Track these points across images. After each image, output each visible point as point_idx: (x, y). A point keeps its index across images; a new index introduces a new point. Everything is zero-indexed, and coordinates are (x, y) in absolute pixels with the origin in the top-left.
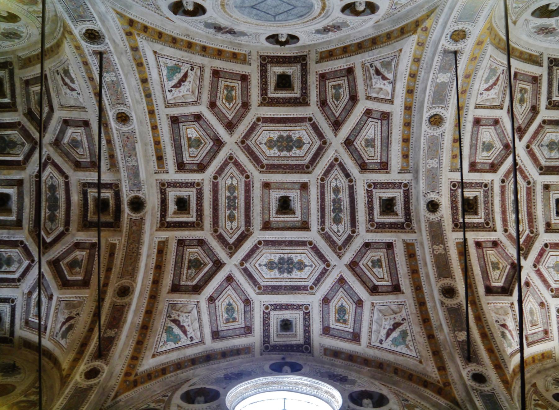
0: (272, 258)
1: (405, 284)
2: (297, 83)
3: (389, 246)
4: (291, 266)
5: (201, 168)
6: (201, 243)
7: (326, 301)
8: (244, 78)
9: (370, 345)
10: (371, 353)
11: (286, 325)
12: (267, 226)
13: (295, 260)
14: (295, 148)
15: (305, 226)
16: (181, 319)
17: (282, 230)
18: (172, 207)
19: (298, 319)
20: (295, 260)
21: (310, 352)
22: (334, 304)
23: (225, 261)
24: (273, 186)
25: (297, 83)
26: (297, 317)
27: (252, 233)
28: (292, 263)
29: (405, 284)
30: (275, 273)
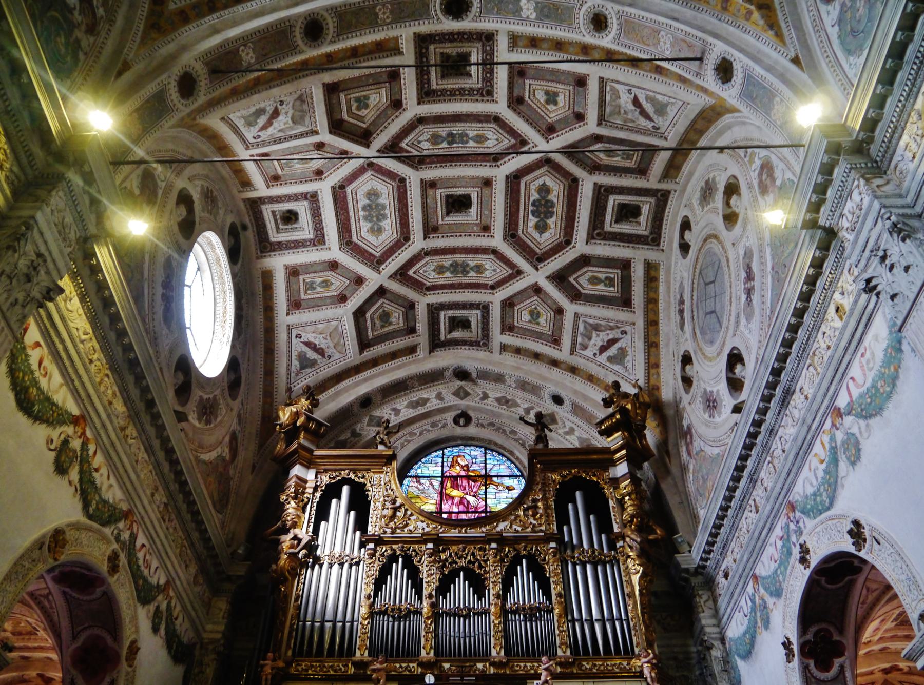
0: (384, 196)
1: (370, 353)
2: (625, 228)
3: (412, 330)
4: (375, 219)
5: (516, 102)
6: (397, 104)
7: (333, 265)
8: (642, 171)
9: (289, 329)
10: (281, 336)
11: (290, 217)
12: (428, 185)
13: (382, 224)
14: (536, 220)
15: (430, 229)
16: (281, 118)
17: (423, 203)
18: (451, 49)
19: (301, 233)
20: (382, 224)
21: (262, 252)
22: (330, 275)
23: (372, 145)
24: (486, 191)
25: (625, 228)
26: (304, 230)
27: (417, 169)
28: (379, 220)
29: (370, 353)
30: (363, 201)
